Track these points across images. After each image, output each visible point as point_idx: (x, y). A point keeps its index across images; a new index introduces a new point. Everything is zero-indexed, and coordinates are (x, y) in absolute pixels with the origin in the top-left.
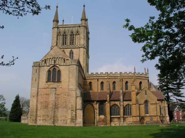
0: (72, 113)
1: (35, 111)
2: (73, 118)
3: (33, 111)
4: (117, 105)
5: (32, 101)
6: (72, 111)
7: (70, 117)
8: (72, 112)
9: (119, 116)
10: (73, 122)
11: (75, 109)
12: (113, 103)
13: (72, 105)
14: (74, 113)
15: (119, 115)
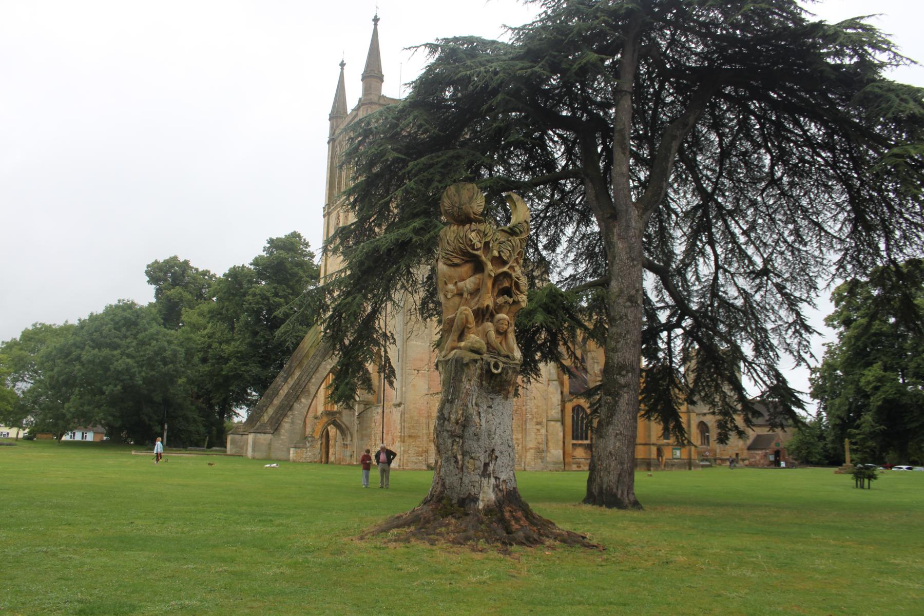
0: (538, 430)
1: (424, 420)
2: (541, 446)
3: (418, 422)
4: (583, 409)
5: (414, 386)
6: (538, 423)
7: (532, 444)
8: (538, 427)
9: (588, 442)
10: (542, 459)
11: (545, 420)
12: (576, 402)
13: (537, 407)
14: (543, 431)
15: (586, 439)
